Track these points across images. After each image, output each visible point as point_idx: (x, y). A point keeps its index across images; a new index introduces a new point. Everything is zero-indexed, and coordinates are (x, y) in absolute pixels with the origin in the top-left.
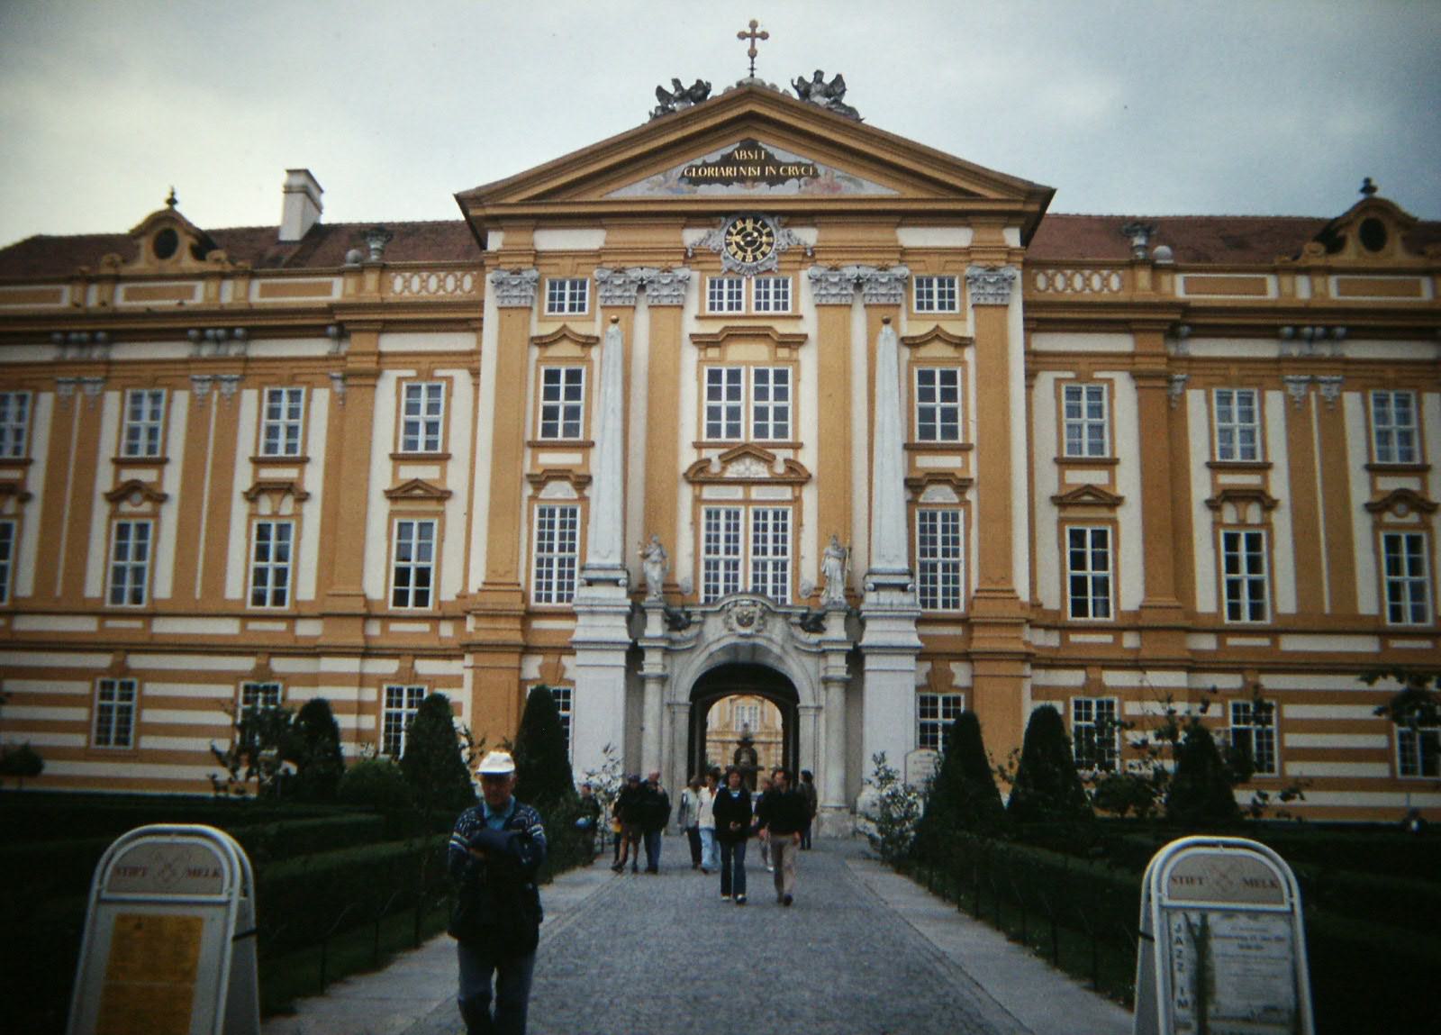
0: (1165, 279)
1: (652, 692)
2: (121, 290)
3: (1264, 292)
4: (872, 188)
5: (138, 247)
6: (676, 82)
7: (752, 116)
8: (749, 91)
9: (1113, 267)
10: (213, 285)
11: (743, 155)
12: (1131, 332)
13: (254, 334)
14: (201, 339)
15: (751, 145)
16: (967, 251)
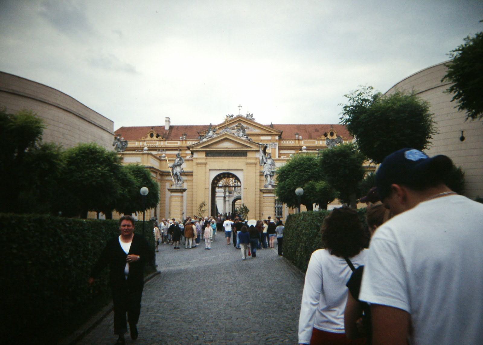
0: (300, 142)
1: (227, 202)
2: (145, 142)
3: (315, 143)
4: (257, 131)
5: (147, 136)
6: (229, 115)
7: (240, 120)
8: (239, 117)
9: (293, 140)
10: (160, 142)
11: (239, 125)
12: (295, 150)
13: (167, 150)
14: (159, 151)
15: (240, 124)
16: (270, 140)
